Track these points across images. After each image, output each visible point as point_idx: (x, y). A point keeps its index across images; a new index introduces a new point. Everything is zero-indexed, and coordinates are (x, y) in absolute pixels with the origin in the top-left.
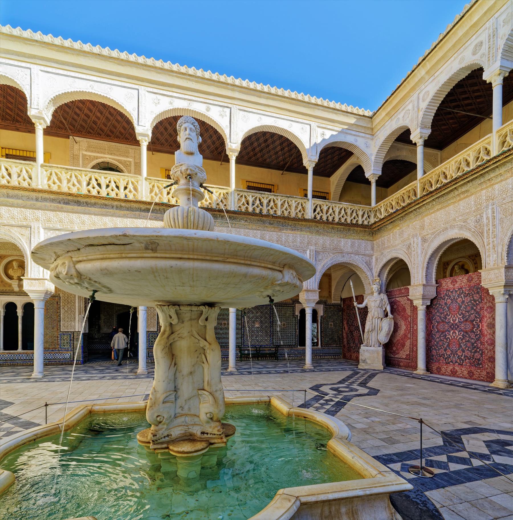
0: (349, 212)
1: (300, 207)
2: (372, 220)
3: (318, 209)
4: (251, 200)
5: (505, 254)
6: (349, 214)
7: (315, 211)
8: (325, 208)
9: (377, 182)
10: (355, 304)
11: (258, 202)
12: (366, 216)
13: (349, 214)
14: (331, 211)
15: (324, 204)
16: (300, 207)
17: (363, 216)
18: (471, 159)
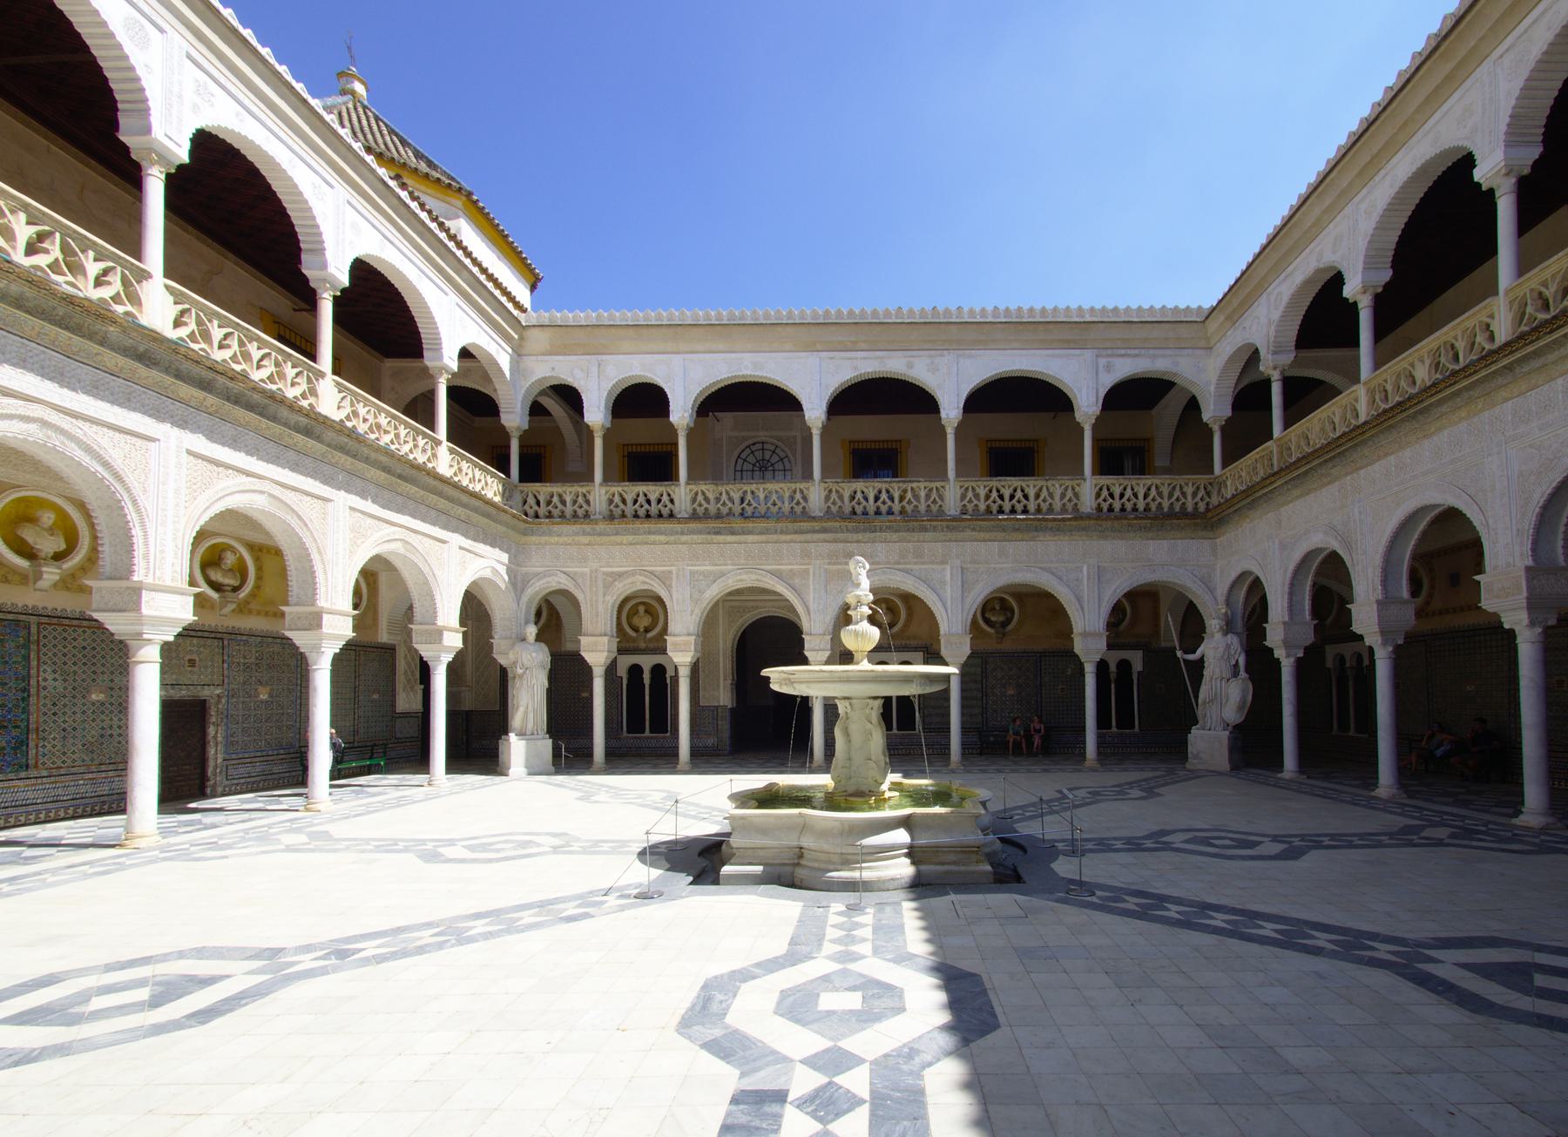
0: (1165, 491)
1: (1069, 494)
2: (1215, 500)
3: (1105, 493)
4: (982, 492)
5: (1378, 581)
6: (1166, 494)
7: (1098, 495)
8: (1117, 491)
9: (1223, 429)
10: (1179, 654)
11: (994, 494)
12: (1202, 493)
13: (1166, 494)
14: (1129, 493)
15: (1116, 483)
16: (1069, 494)
17: (1195, 494)
18: (1461, 346)
